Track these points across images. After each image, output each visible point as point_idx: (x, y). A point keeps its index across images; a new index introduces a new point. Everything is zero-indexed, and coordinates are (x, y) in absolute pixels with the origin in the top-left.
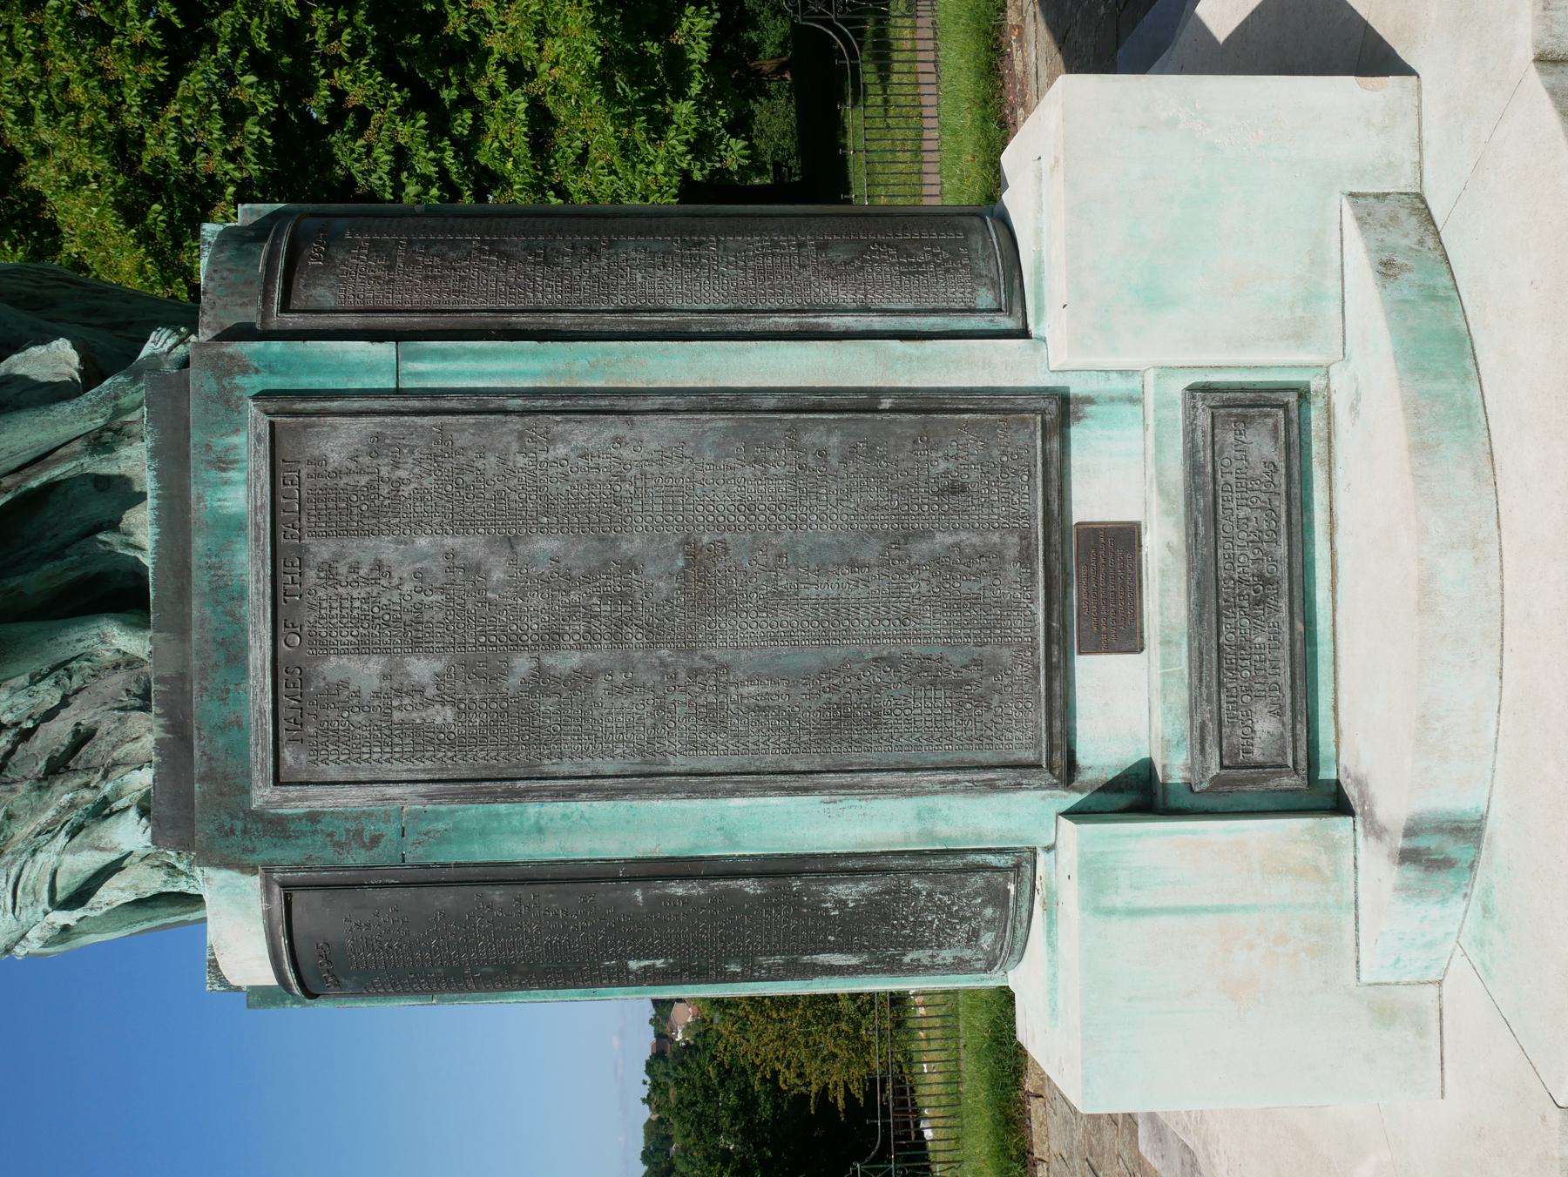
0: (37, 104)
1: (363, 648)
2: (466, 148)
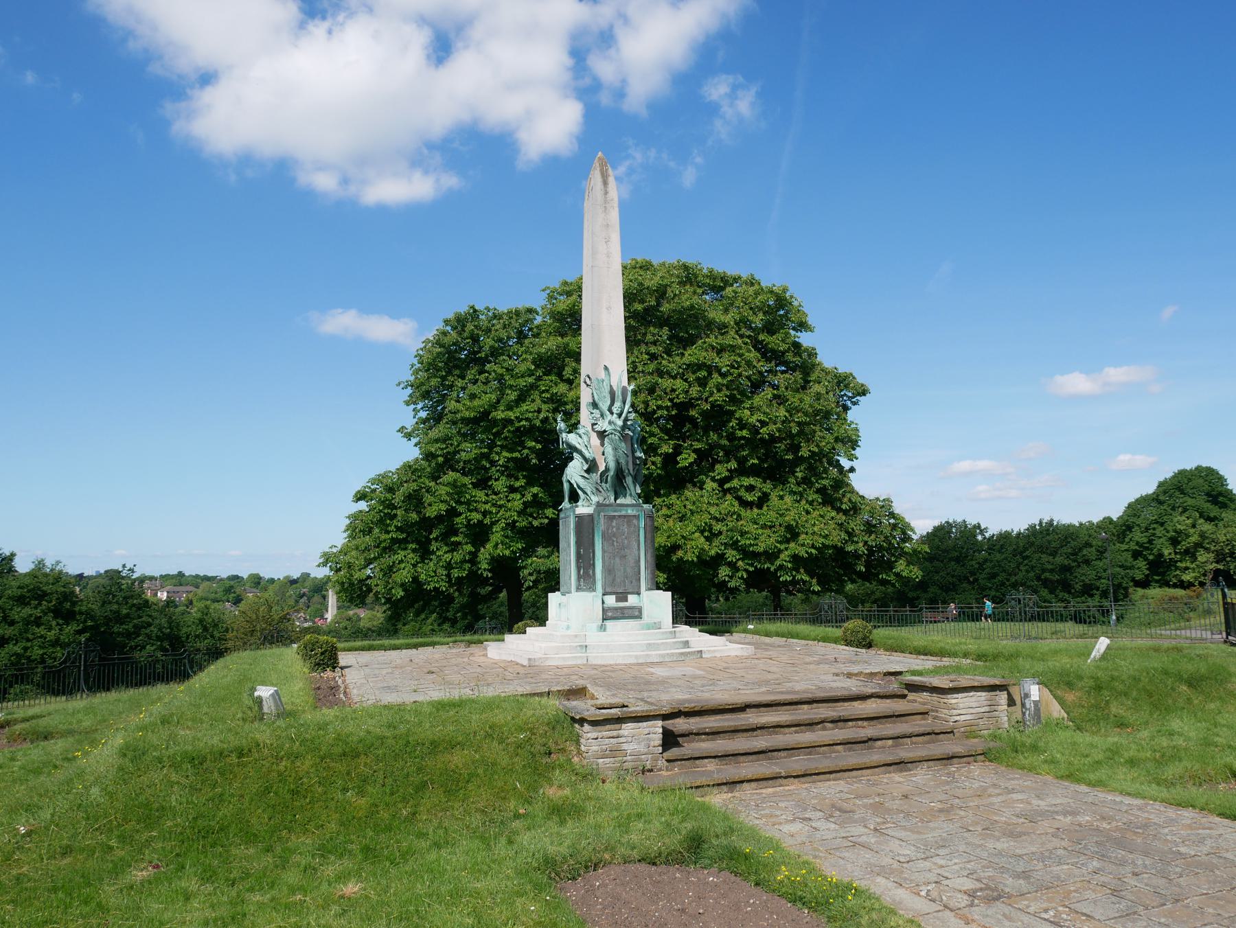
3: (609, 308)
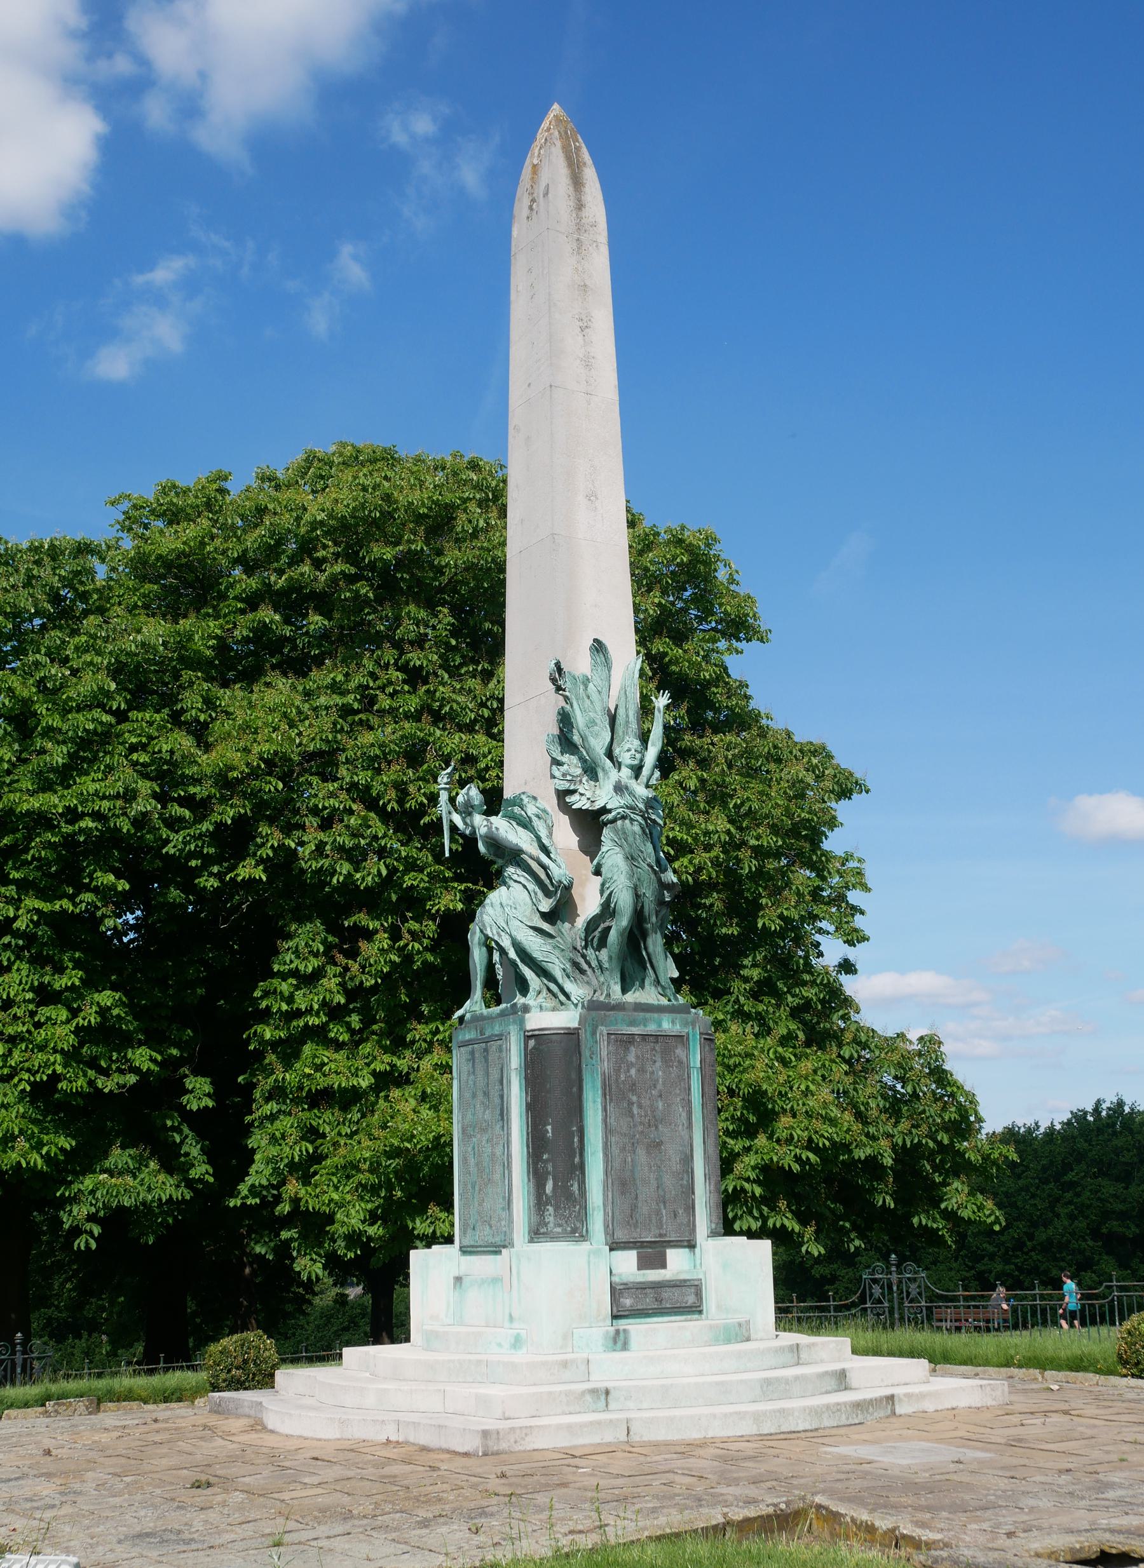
0: (350, 699)
1: (637, 1057)
2: (319, 1034)
3: (591, 497)
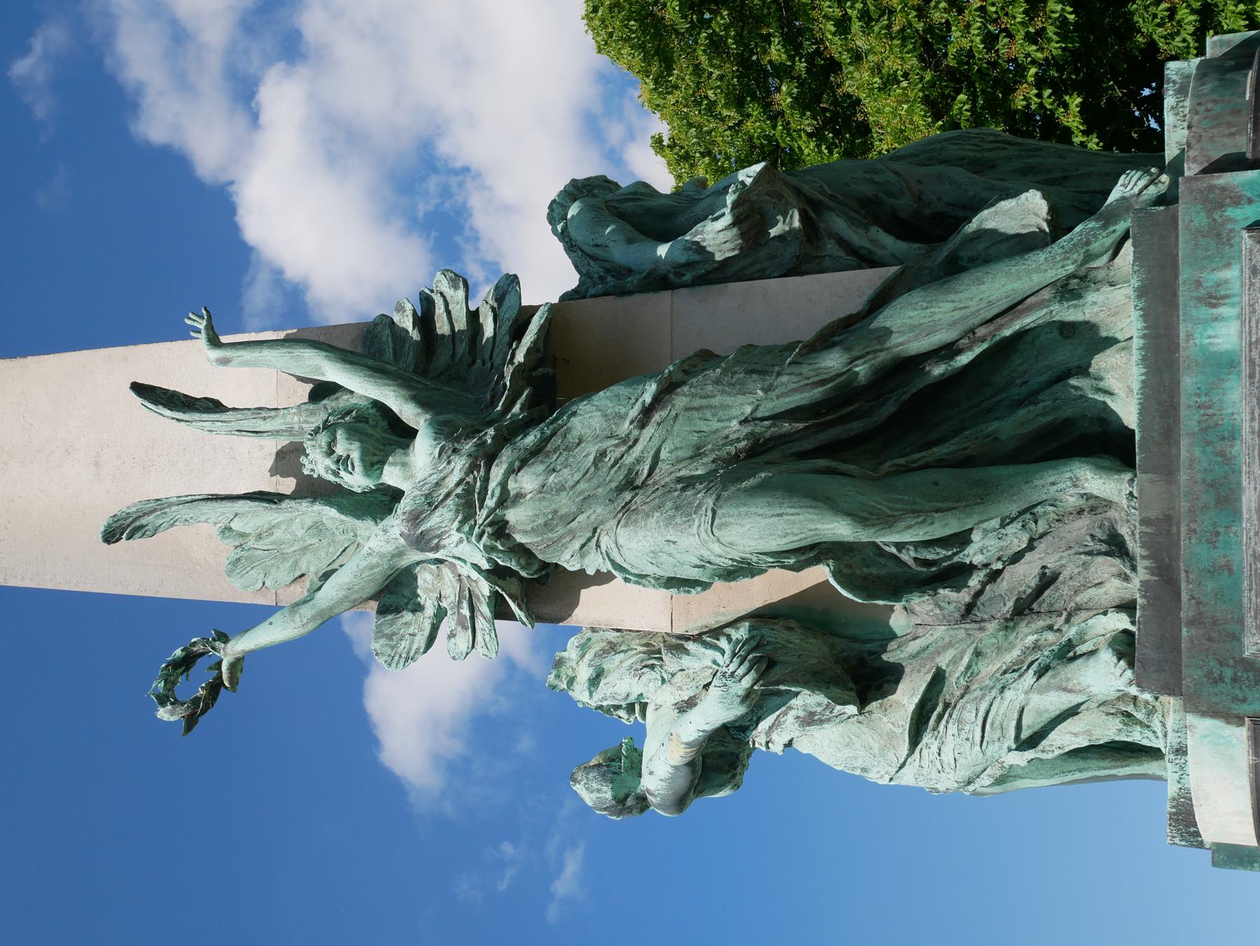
0: (853, 13)
